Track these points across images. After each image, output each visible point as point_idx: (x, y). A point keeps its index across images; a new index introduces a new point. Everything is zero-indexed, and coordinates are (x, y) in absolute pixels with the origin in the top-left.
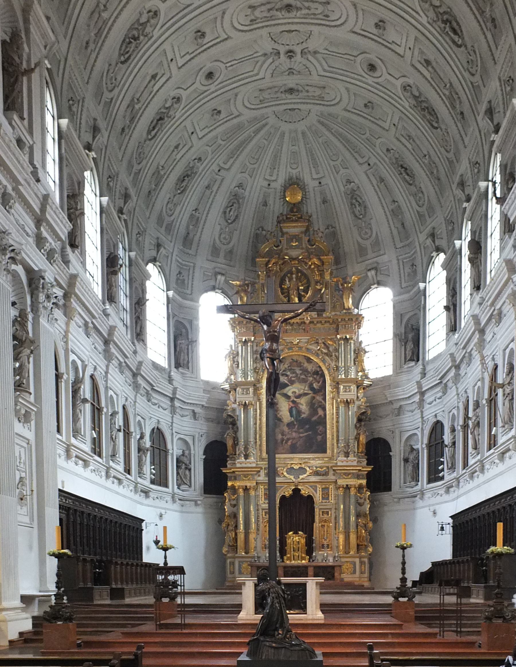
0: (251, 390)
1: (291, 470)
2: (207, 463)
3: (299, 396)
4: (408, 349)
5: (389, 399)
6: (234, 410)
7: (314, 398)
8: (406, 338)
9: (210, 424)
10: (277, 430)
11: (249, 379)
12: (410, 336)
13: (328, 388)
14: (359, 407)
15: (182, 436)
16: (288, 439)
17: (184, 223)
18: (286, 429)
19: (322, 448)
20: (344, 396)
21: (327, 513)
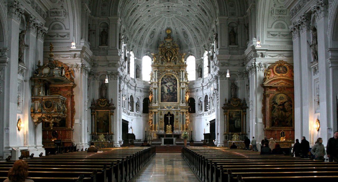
0: (157, 84)
1: (167, 107)
2: (144, 104)
3: (170, 86)
4: (199, 74)
5: (194, 87)
6: (152, 90)
7: (174, 86)
8: (199, 71)
9: (145, 93)
10: (164, 95)
11: (156, 81)
12: (200, 70)
13: (178, 84)
14: (186, 90)
15: (137, 97)
16: (167, 98)
17: (139, 39)
18: (166, 95)
19: (176, 101)
20: (182, 86)
21: (178, 119)
